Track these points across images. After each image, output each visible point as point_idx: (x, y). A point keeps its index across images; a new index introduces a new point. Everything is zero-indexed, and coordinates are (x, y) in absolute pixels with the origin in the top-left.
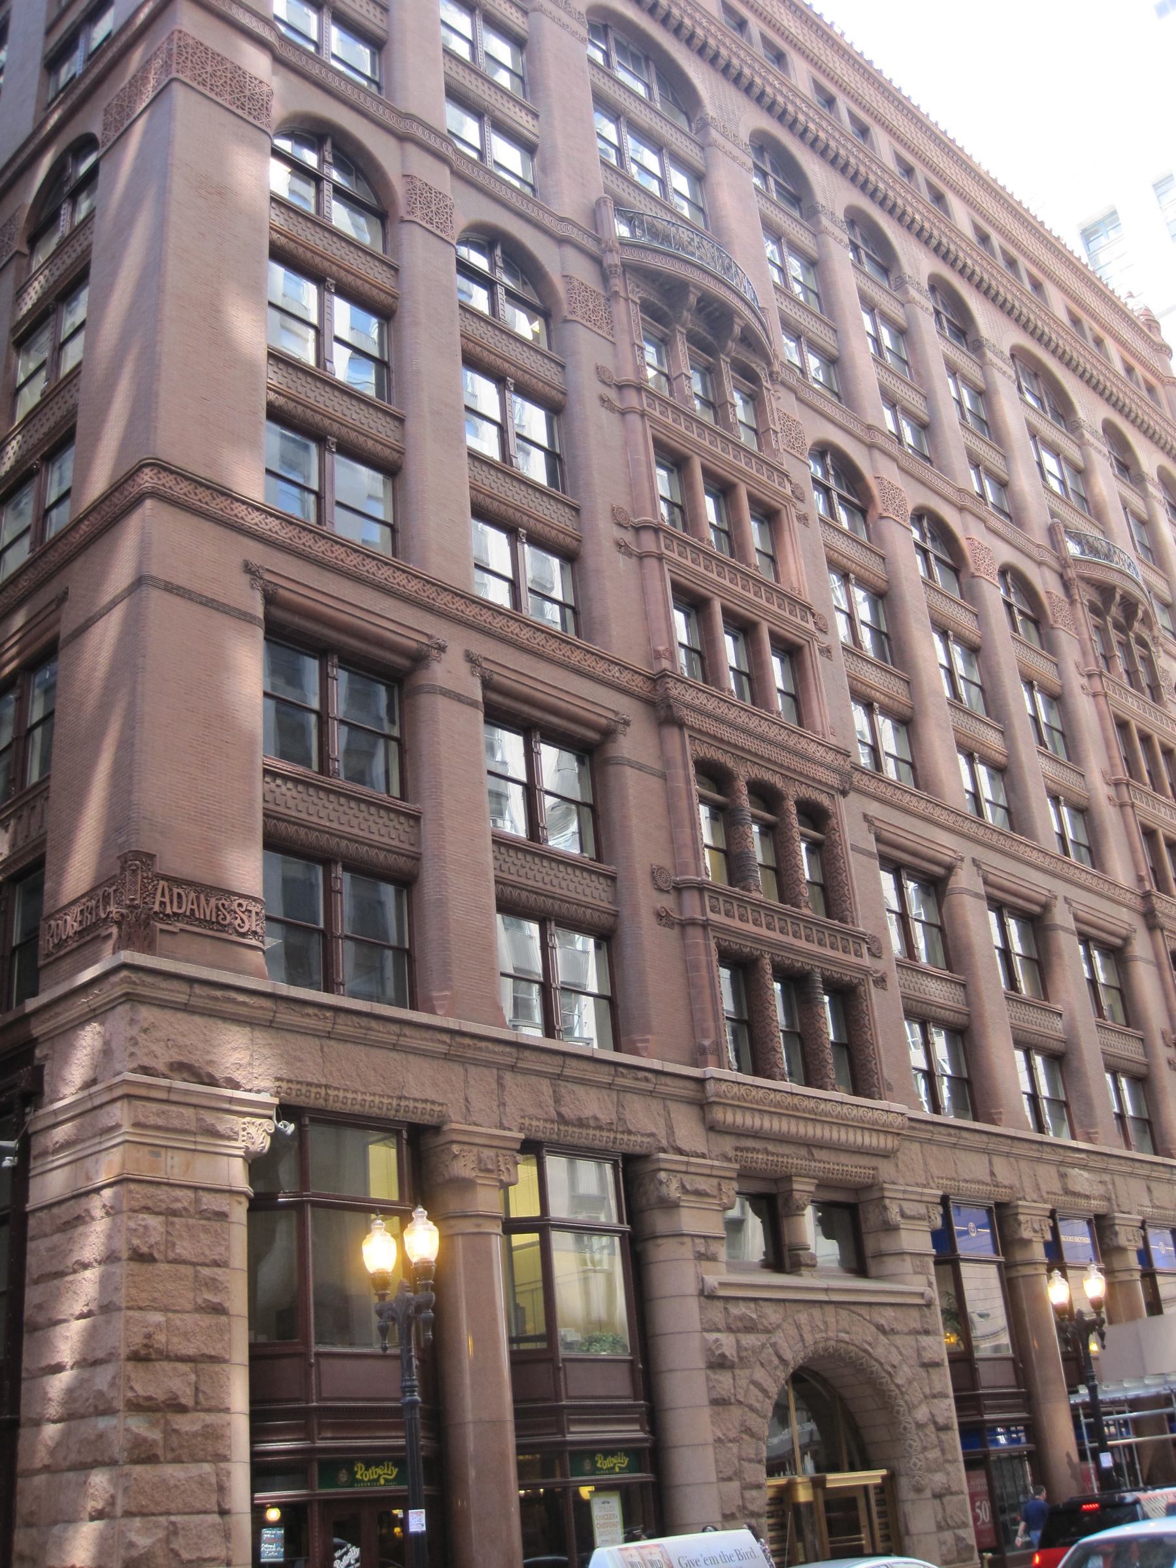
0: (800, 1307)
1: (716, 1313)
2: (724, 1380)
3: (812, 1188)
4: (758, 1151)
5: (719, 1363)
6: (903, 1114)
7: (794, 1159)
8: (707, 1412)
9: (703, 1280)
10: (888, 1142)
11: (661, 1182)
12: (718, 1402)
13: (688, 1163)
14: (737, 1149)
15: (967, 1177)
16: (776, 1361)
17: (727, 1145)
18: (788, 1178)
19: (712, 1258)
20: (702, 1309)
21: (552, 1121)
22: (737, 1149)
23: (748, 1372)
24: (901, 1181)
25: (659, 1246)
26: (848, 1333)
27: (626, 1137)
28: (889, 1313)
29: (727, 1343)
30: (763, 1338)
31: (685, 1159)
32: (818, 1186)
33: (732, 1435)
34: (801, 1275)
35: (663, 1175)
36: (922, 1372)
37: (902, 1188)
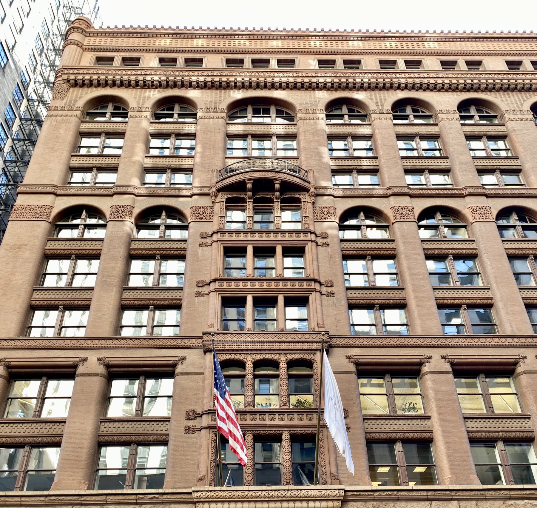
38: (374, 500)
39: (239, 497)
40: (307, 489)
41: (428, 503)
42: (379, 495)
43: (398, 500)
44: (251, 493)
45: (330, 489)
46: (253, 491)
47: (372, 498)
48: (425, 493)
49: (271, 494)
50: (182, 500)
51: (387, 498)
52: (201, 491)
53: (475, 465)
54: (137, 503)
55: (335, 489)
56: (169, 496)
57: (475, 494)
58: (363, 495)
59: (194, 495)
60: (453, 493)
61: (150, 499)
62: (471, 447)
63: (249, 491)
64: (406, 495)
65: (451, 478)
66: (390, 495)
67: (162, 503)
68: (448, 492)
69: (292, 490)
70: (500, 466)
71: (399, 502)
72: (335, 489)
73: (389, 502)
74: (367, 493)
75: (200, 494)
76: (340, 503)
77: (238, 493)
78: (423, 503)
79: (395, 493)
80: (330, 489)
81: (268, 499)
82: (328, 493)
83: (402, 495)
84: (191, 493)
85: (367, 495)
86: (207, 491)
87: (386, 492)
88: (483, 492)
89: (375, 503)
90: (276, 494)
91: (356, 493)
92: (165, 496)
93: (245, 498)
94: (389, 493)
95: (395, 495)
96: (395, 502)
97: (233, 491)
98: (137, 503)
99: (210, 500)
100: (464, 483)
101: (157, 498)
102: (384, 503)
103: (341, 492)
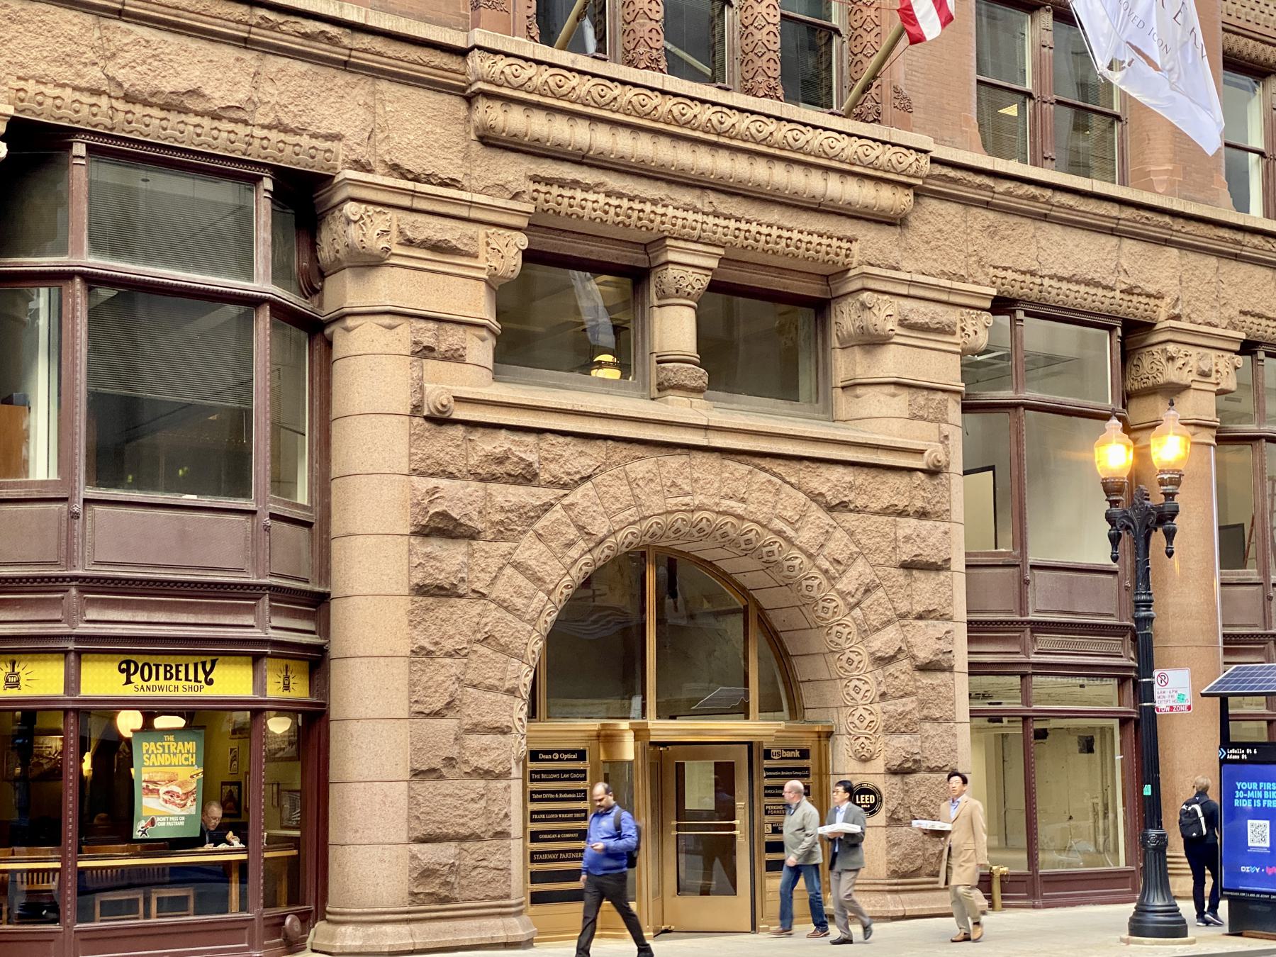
0: (638, 451)
1: (446, 444)
2: (450, 558)
3: (713, 263)
4: (587, 188)
5: (441, 528)
6: (926, 152)
7: (672, 210)
8: (405, 604)
9: (422, 388)
10: (887, 198)
11: (349, 221)
12: (433, 592)
13: (414, 194)
14: (536, 179)
15: (1061, 272)
16: (572, 533)
17: (514, 170)
18: (660, 242)
19: (455, 357)
20: (415, 438)
21: (96, 92)
22: (536, 179)
23: (505, 547)
24: (905, 264)
25: (348, 330)
26: (743, 500)
27: (274, 135)
28: (838, 473)
29: (459, 497)
30: (547, 495)
31: (410, 185)
32: (723, 260)
33: (449, 645)
34: (667, 402)
35: (350, 209)
36: (899, 576)
37: (908, 277)
38: (987, 205)
39: (630, 109)
40: (822, 129)
41: (1115, 240)
42: (1008, 193)
43: (1045, 218)
44: (670, 103)
45: (894, 145)
46: (676, 95)
47: (984, 196)
48: (1114, 210)
49: (728, 122)
50: (423, 72)
51: (1025, 205)
52: (508, 55)
53: (1227, 145)
54: (246, 43)
55: (908, 148)
56: (378, 44)
57: (1222, 239)
58: (969, 185)
59: (477, 63)
60: (1178, 224)
61: (305, 36)
62: (1225, 82)
63: (664, 93)
64: (1071, 208)
65: (1172, 172)
66: (1034, 198)
67: (345, 66)
68: (1167, 219)
69: (789, 121)
70: (1253, 157)
71: (1045, 226)
72: (908, 148)
73: (1024, 220)
74: (979, 179)
75: (502, 63)
76: (911, 197)
77: (630, 93)
78: (1103, 239)
79: (1048, 193)
80: (894, 145)
81: (714, 138)
82: (888, 154)
83: (1062, 206)
84: (462, 53)
85: (979, 186)
86: (527, 60)
87: (1026, 187)
88: (1239, 236)
89: (991, 215)
90: (744, 123)
91: (952, 173)
92: (366, 41)
93: (646, 115)
94: (1033, 190)
95: (1047, 202)
96: (1038, 224)
97: (612, 80)
98: (245, 40)
99: (535, 98)
100: (1198, 196)
101: (331, 40)
102: (1013, 220)
103: (922, 162)
